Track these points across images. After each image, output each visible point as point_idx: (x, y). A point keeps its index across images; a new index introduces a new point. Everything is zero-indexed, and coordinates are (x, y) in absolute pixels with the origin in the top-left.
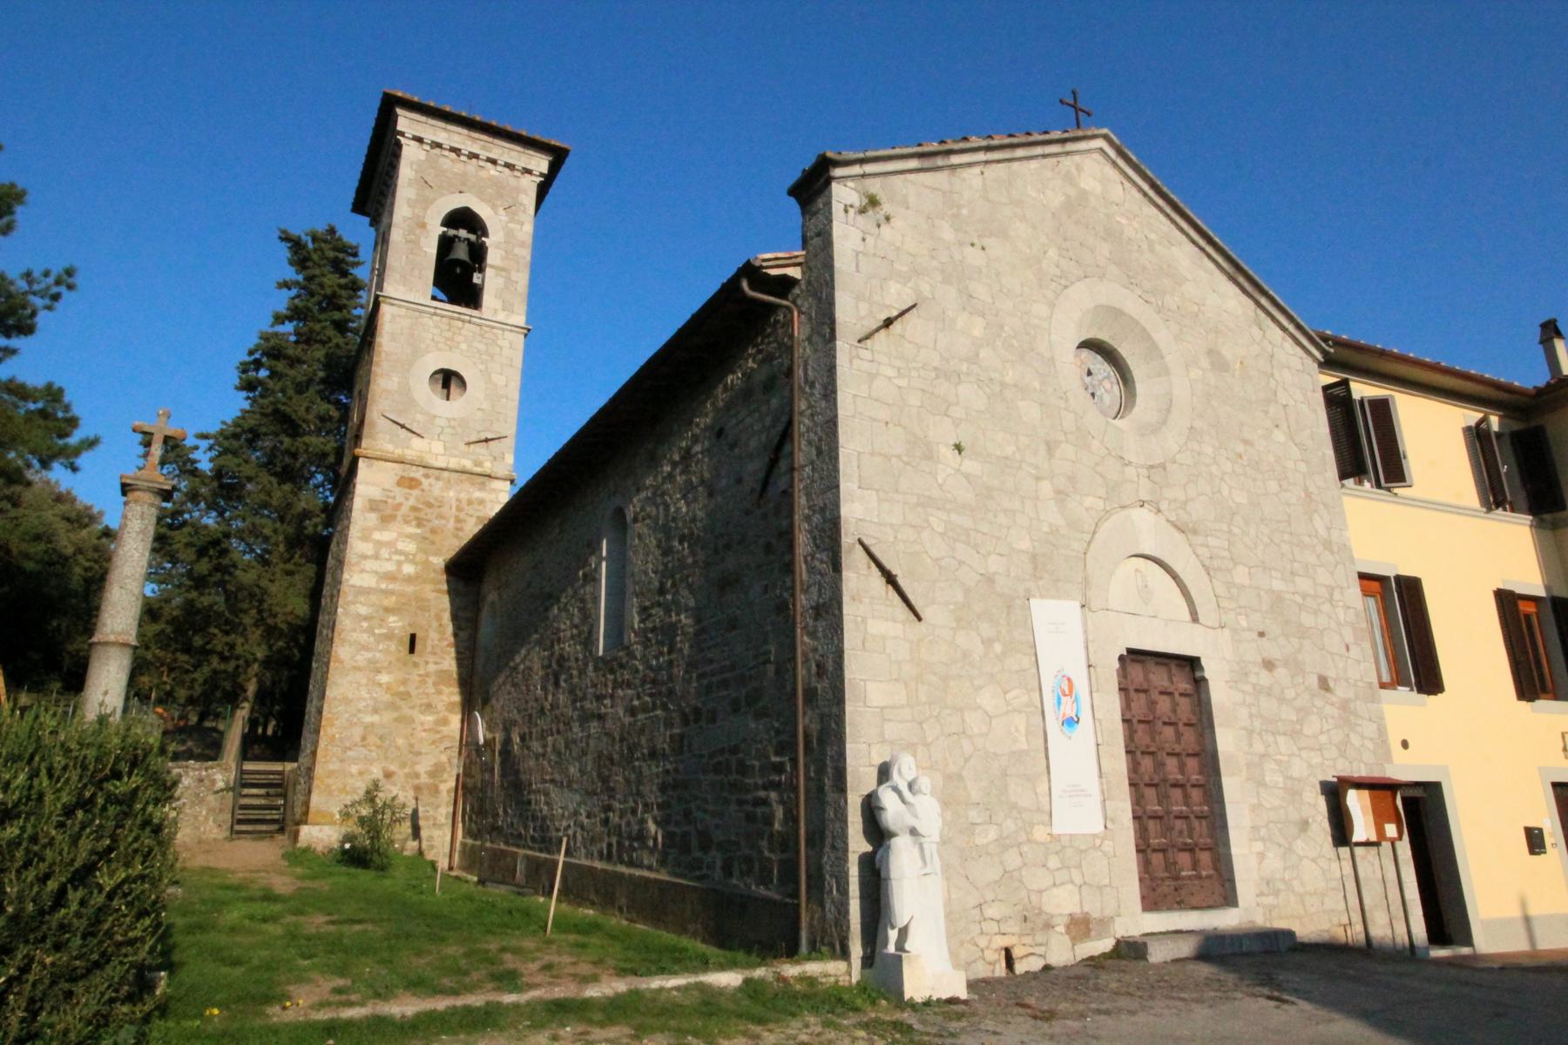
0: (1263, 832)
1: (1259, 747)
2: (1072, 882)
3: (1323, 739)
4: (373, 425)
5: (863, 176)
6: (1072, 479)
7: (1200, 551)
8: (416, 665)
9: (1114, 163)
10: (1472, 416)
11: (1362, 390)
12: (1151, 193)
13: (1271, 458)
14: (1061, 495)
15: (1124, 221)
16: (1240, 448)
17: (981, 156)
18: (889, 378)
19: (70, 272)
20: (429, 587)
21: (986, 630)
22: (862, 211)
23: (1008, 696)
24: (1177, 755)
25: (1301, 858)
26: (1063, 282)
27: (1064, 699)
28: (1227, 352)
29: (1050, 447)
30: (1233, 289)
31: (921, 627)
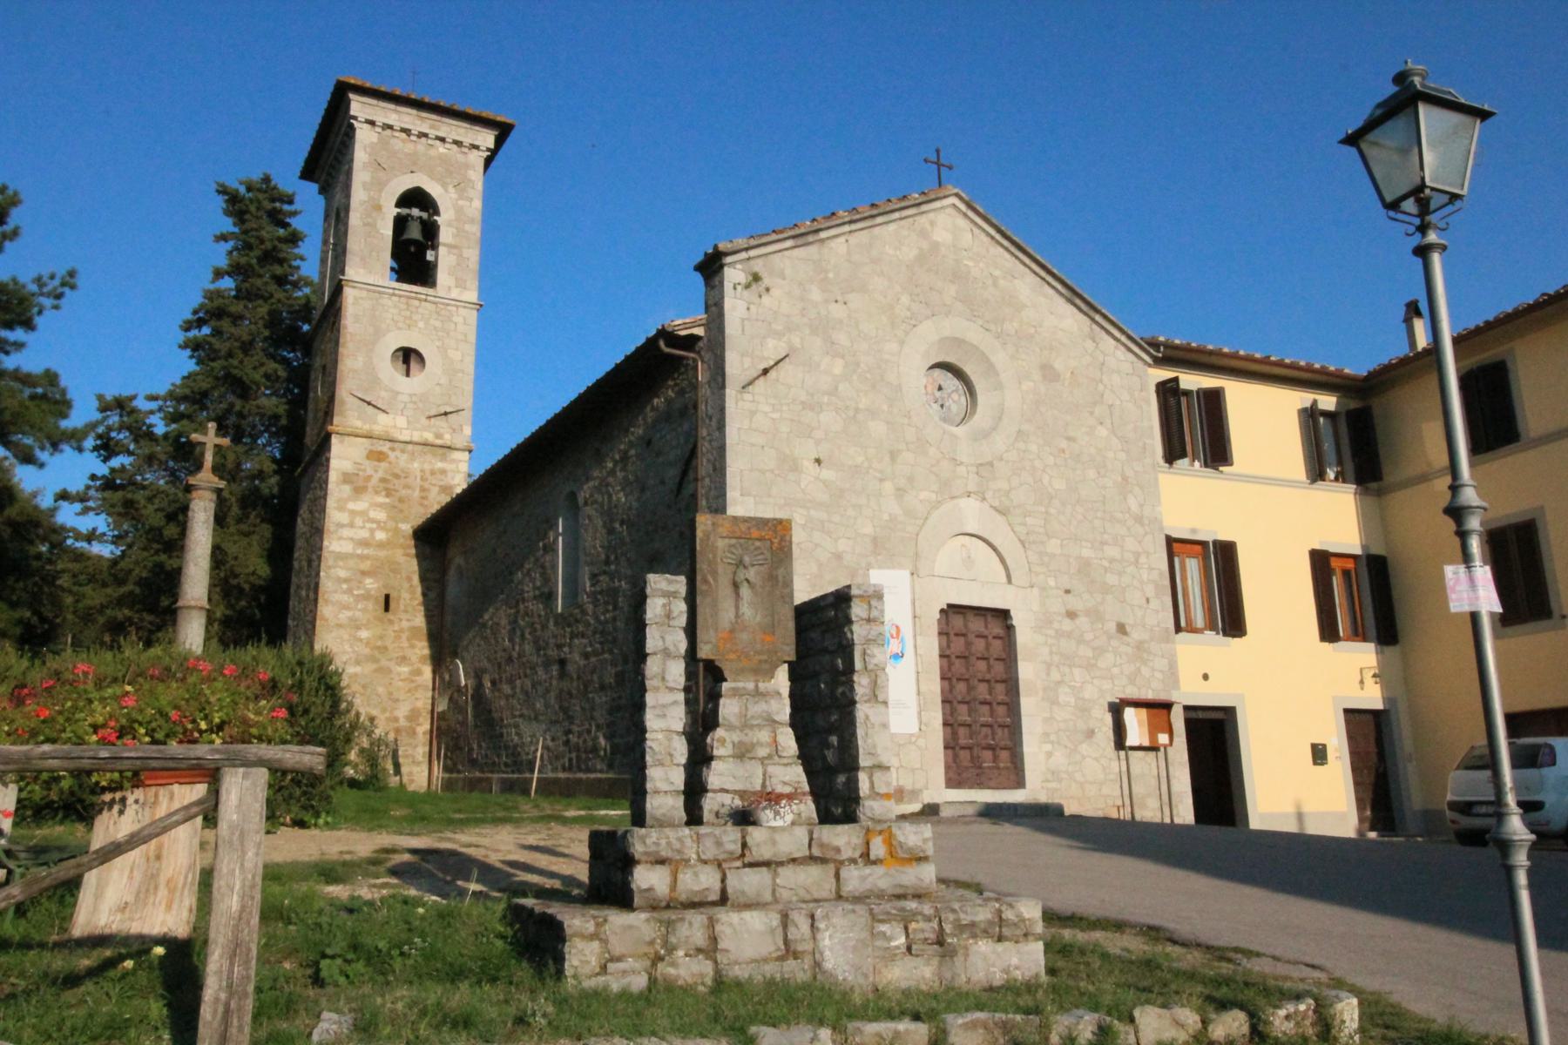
0: (1053, 737)
1: (1055, 676)
3: (1116, 670)
4: (343, 402)
6: (911, 479)
7: (1017, 528)
8: (391, 622)
9: (965, 215)
10: (1301, 398)
12: (998, 237)
13: (1093, 451)
14: (900, 492)
15: (971, 264)
16: (1064, 444)
17: (847, 228)
19: (72, 274)
20: (399, 552)
22: (747, 286)
24: (988, 681)
25: (1084, 757)
28: (1058, 365)
29: (893, 455)
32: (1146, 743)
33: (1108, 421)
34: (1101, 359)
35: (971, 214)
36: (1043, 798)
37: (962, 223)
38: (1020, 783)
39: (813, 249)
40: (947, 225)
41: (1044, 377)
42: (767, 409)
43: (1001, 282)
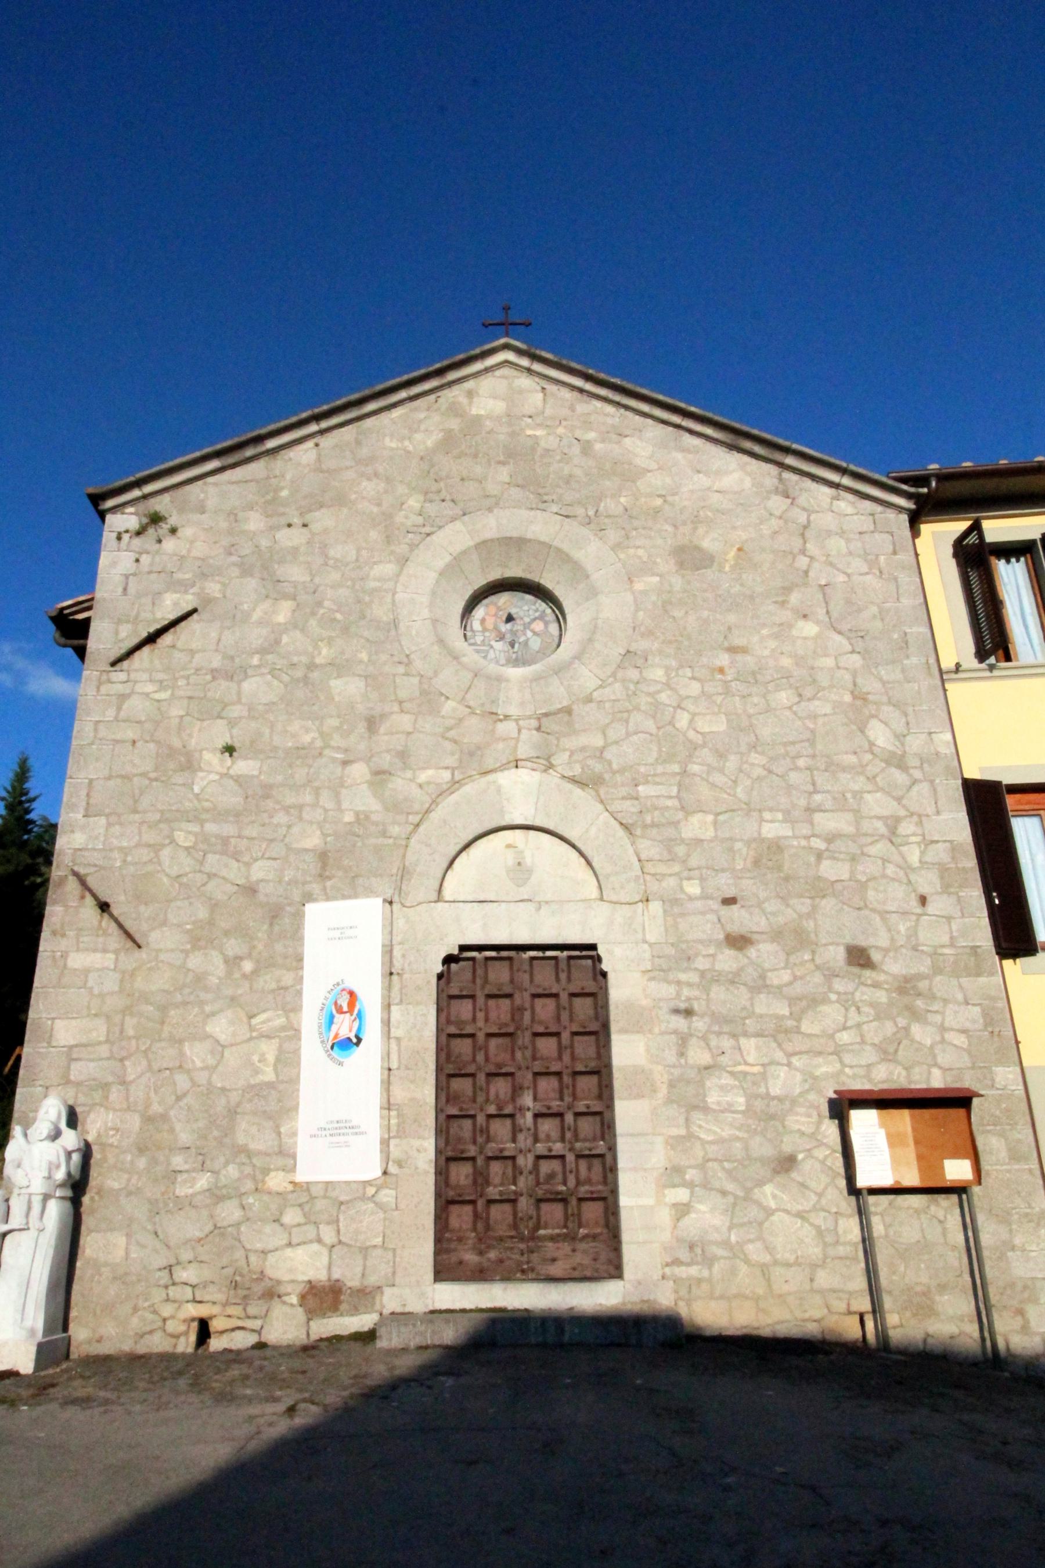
0: (690, 1174)
1: (698, 1055)
2: (319, 1241)
3: (845, 1037)
5: (145, 497)
6: (403, 755)
11: (999, 528)
12: (589, 387)
14: (380, 776)
15: (539, 433)
16: (723, 659)
17: (313, 428)
18: (147, 695)
21: (233, 946)
23: (254, 1021)
25: (769, 1212)
26: (427, 530)
27: (338, 1018)
29: (372, 724)
30: (736, 459)
31: (143, 954)
32: (912, 1179)
33: (821, 612)
34: (803, 518)
35: (537, 367)
36: (664, 1299)
37: (525, 382)
38: (615, 1270)
39: (256, 469)
40: (505, 394)
41: (681, 565)
42: (149, 688)
43: (598, 446)
